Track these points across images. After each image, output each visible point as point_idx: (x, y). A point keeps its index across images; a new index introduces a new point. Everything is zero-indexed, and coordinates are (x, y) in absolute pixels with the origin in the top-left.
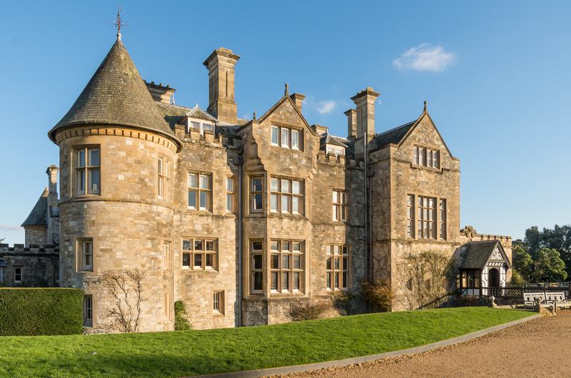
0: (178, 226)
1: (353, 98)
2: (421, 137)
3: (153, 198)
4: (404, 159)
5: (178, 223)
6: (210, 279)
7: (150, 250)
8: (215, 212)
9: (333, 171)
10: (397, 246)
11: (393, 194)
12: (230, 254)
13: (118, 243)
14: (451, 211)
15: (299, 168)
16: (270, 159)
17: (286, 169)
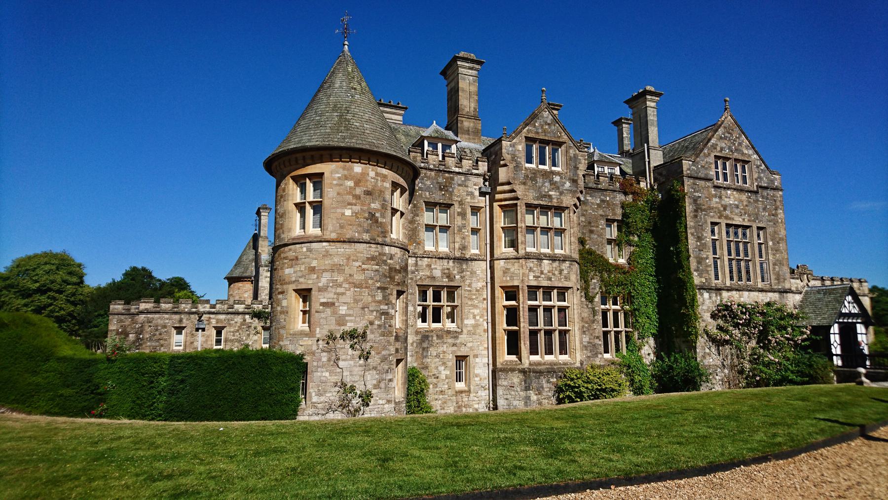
0: (413, 272)
1: (626, 102)
2: (724, 145)
3: (385, 237)
4: (703, 176)
5: (413, 268)
6: (451, 341)
7: (380, 302)
8: (458, 254)
9: (606, 196)
10: (702, 295)
11: (690, 223)
12: (475, 307)
13: (343, 294)
14: (774, 244)
15: (561, 193)
16: (524, 184)
17: (545, 196)
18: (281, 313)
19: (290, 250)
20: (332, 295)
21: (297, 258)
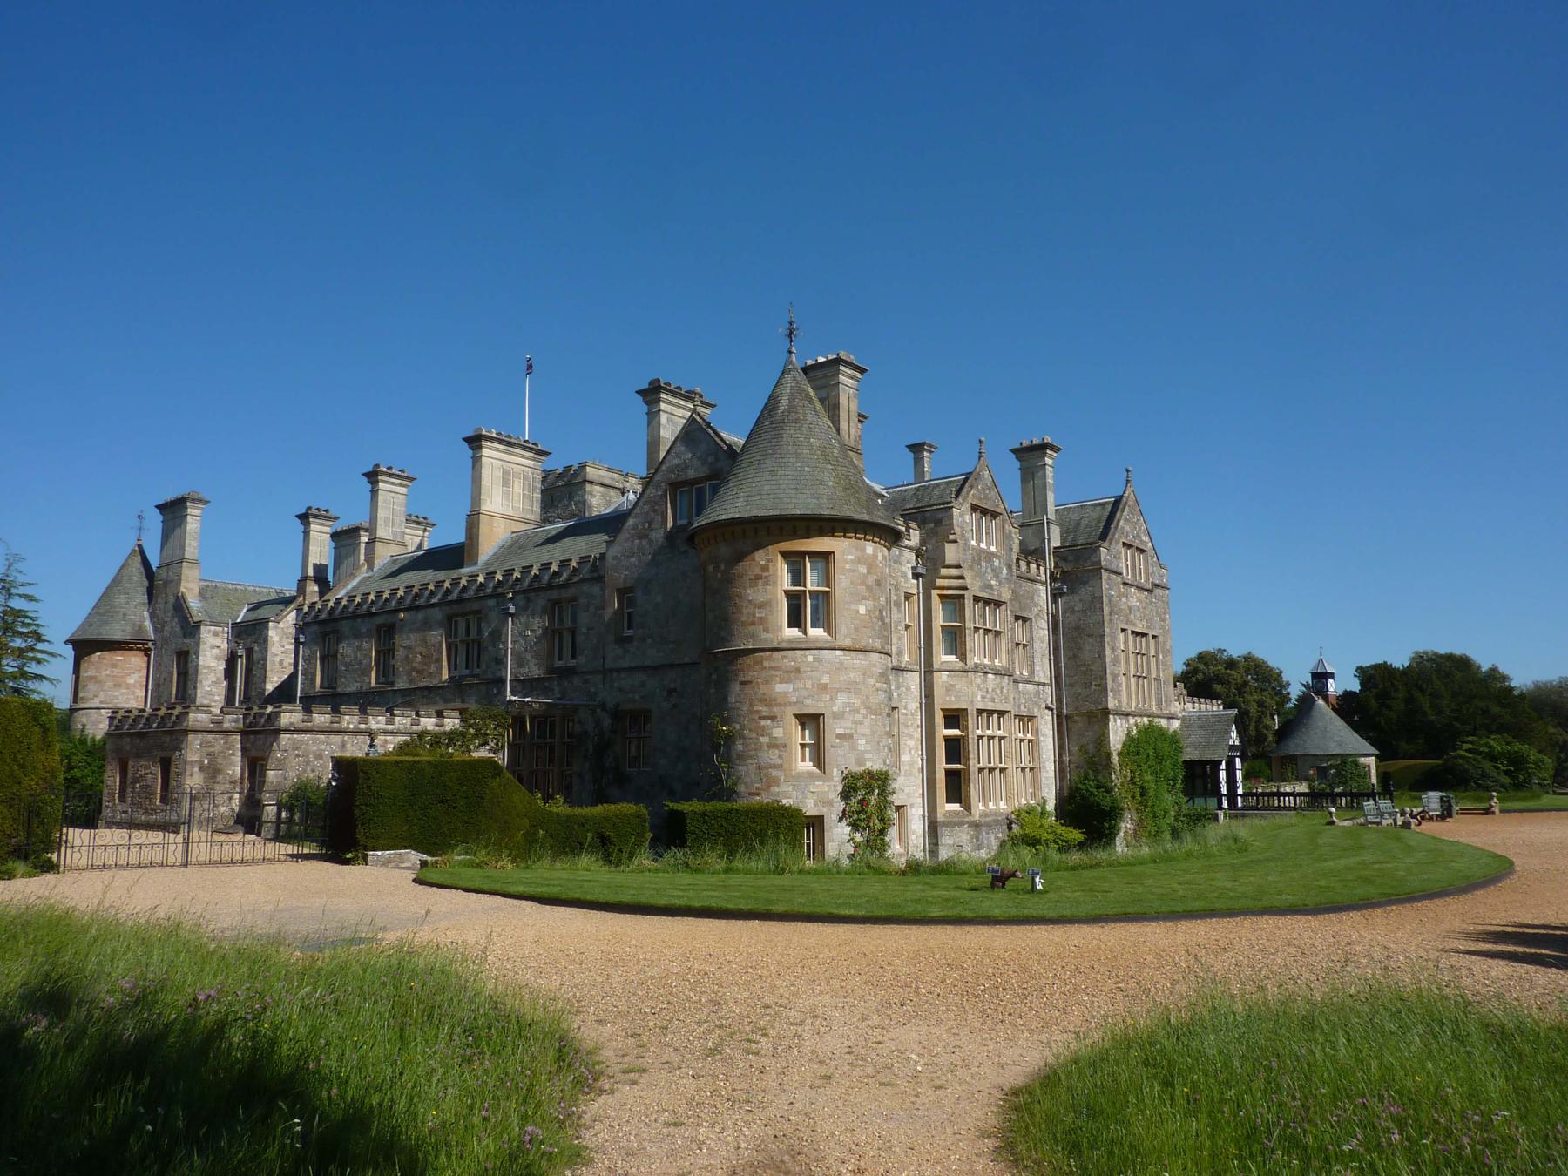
1: (1014, 451)
13: (861, 723)
16: (971, 568)
18: (770, 746)
19: (784, 657)
20: (849, 724)
21: (798, 670)
